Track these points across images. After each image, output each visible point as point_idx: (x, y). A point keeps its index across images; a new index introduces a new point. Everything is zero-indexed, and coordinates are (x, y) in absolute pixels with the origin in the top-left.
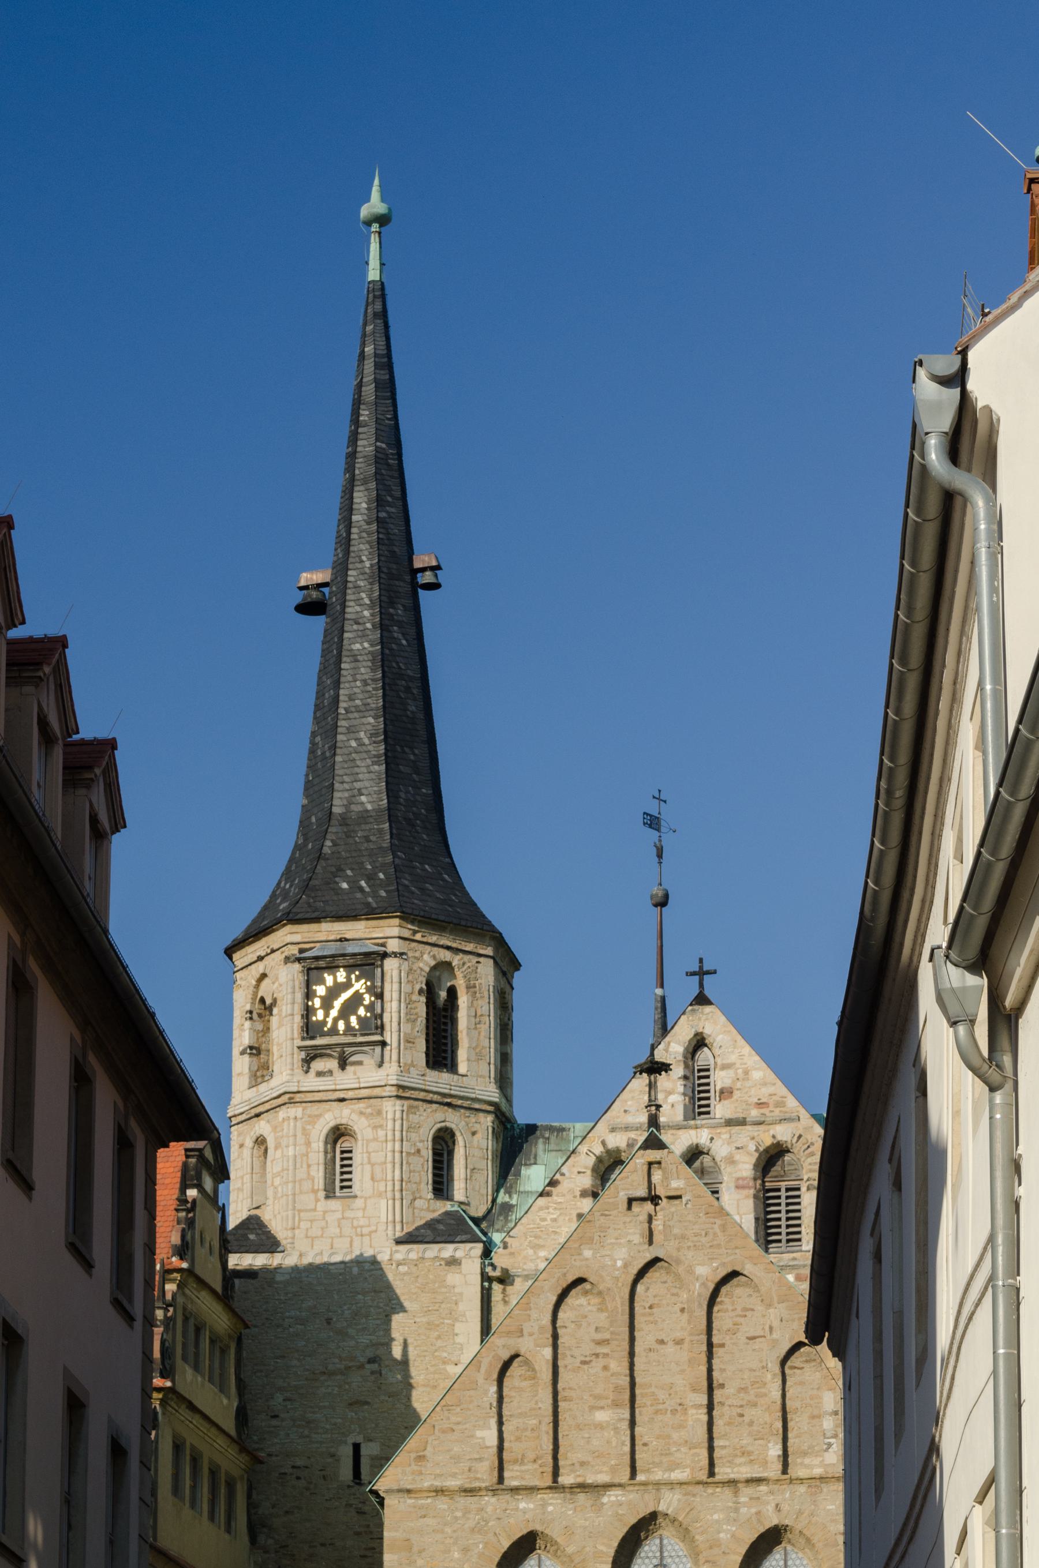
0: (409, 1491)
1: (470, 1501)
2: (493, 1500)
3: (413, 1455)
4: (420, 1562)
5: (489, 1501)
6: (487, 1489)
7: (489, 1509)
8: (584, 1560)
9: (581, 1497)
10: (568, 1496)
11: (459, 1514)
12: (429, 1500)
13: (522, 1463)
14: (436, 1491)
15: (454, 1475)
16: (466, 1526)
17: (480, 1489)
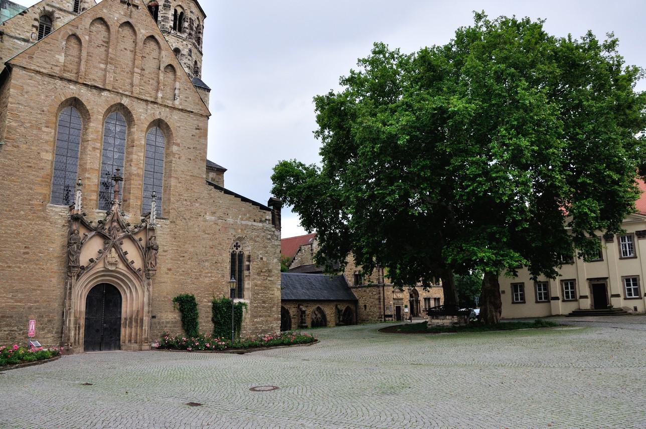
0: (25, 68)
1: (52, 81)
2: (60, 82)
3: (27, 55)
4: (26, 96)
5: (58, 82)
6: (59, 77)
7: (58, 84)
8: (93, 113)
9: (94, 91)
10: (89, 89)
11: (45, 83)
12: (33, 74)
13: (71, 73)
14: (37, 71)
15: (45, 68)
16: (48, 88)
17: (56, 76)
